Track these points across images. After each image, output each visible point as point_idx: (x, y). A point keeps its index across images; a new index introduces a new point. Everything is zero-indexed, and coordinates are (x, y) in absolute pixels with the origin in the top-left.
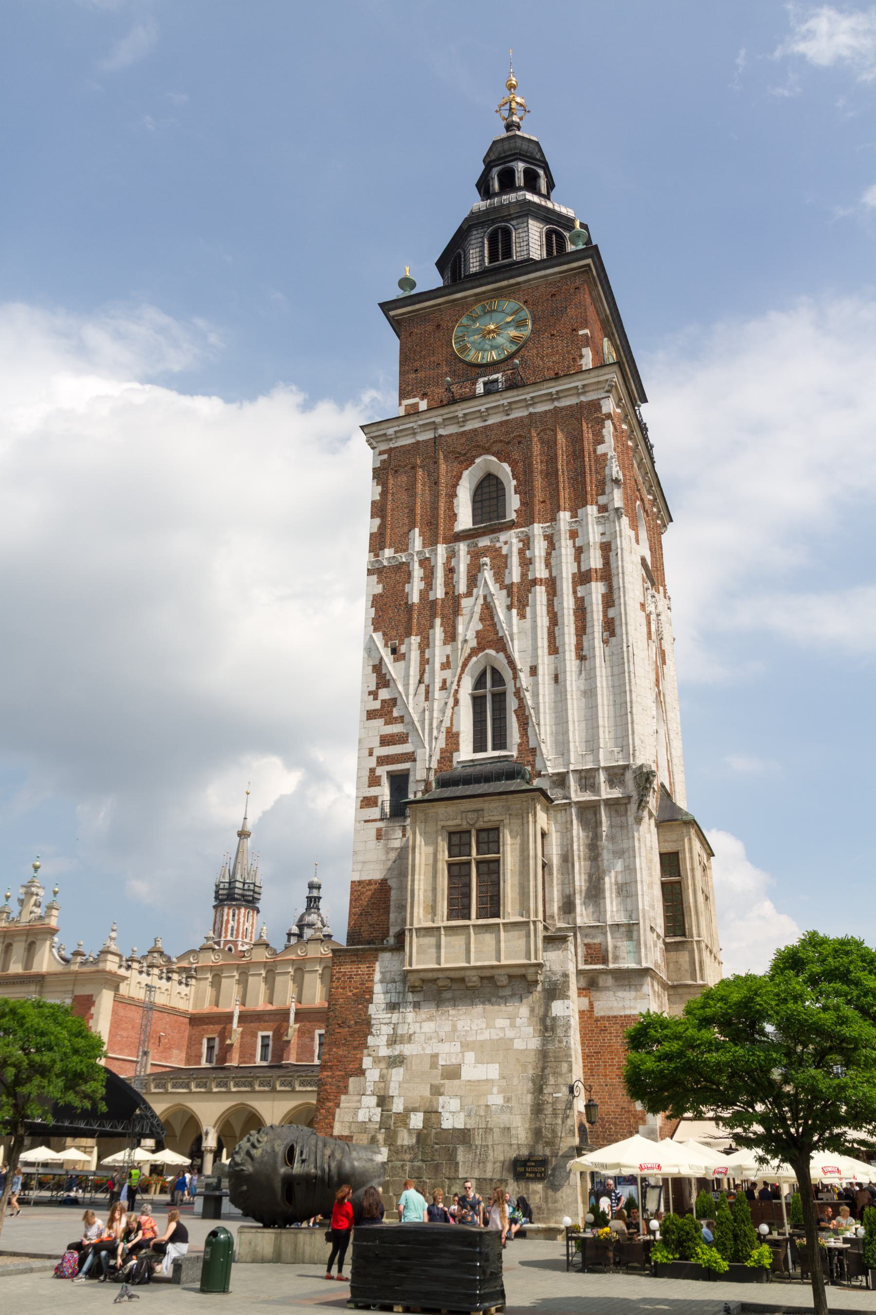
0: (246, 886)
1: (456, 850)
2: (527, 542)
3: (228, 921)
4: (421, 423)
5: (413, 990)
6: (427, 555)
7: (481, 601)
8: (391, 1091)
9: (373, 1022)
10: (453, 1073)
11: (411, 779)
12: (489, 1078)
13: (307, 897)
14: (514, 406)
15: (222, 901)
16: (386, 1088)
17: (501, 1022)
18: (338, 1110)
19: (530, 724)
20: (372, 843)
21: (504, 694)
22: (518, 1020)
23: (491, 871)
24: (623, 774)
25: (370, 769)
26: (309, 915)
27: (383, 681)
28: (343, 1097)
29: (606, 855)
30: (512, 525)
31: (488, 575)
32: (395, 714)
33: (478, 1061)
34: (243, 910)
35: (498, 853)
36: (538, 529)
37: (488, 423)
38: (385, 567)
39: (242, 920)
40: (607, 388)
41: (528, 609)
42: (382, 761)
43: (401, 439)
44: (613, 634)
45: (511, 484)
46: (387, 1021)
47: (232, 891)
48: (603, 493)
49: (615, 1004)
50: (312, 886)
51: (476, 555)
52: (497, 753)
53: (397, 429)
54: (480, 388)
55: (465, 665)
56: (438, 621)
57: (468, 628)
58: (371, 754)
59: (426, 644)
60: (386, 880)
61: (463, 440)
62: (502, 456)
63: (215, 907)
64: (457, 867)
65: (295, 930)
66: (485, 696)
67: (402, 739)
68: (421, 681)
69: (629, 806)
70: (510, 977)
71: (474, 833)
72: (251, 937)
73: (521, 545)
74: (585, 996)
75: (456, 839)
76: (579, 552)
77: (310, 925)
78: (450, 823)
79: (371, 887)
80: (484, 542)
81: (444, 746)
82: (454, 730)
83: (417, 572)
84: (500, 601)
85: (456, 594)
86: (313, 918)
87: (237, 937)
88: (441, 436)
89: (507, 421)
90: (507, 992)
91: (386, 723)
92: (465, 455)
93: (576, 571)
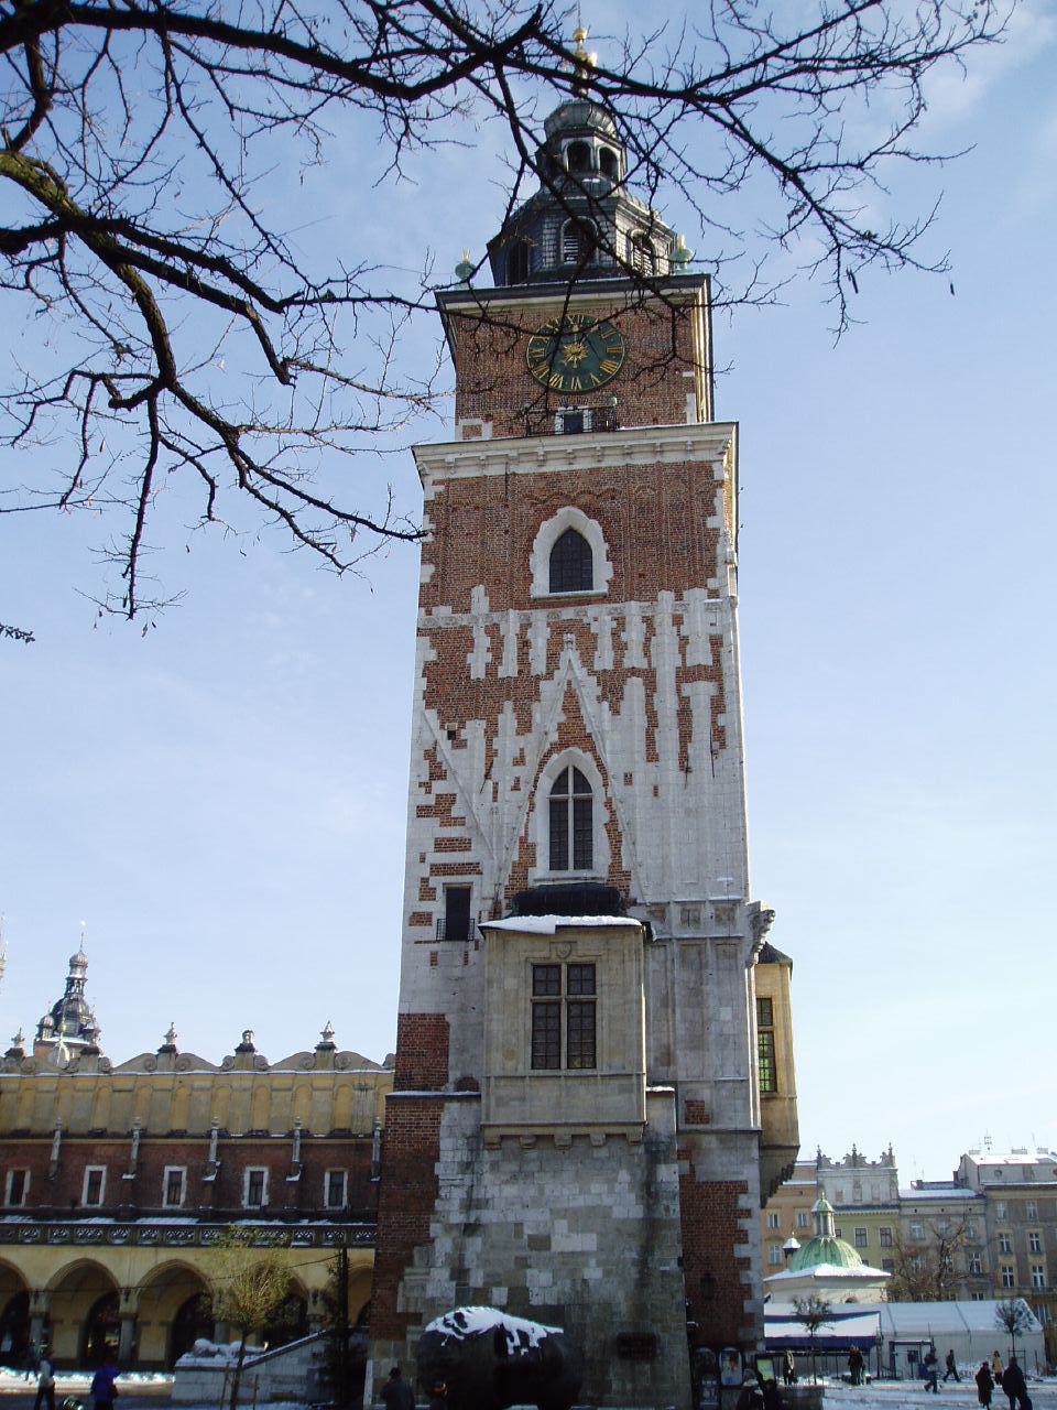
1: (541, 988)
2: (621, 623)
4: (489, 453)
5: (491, 1146)
6: (496, 621)
7: (565, 688)
8: (466, 1263)
9: (441, 1183)
10: (541, 1243)
11: (475, 895)
12: (585, 1248)
13: (68, 979)
14: (607, 452)
16: (461, 1259)
17: (596, 1188)
18: (401, 1284)
19: (624, 842)
20: (425, 968)
21: (590, 801)
22: (617, 1185)
23: (585, 1015)
24: (732, 910)
25: (422, 879)
27: (437, 773)
28: (408, 1270)
29: (711, 1002)
30: (604, 599)
31: (571, 655)
32: (453, 814)
33: (570, 1230)
35: (594, 993)
36: (634, 610)
37: (576, 467)
38: (440, 628)
40: (720, 450)
41: (622, 703)
42: (437, 869)
43: (462, 469)
44: (723, 746)
45: (599, 548)
46: (457, 1182)
48: (714, 575)
49: (720, 1168)
50: (74, 964)
51: (558, 630)
52: (584, 873)
53: (458, 456)
55: (542, 763)
56: (508, 706)
57: (548, 715)
58: (423, 860)
60: (443, 1015)
61: (542, 484)
62: (592, 512)
64: (544, 1007)
66: (567, 801)
67: (463, 845)
68: (487, 776)
69: (738, 948)
70: (608, 1136)
71: (564, 968)
73: (614, 624)
74: (687, 1159)
75: (541, 974)
76: (684, 641)
78: (536, 954)
79: (425, 1022)
80: (568, 614)
81: (516, 859)
82: (530, 840)
83: (483, 641)
84: (589, 690)
85: (533, 673)
88: (514, 474)
89: (599, 468)
90: (603, 1153)
91: (443, 824)
92: (545, 501)
93: (679, 663)
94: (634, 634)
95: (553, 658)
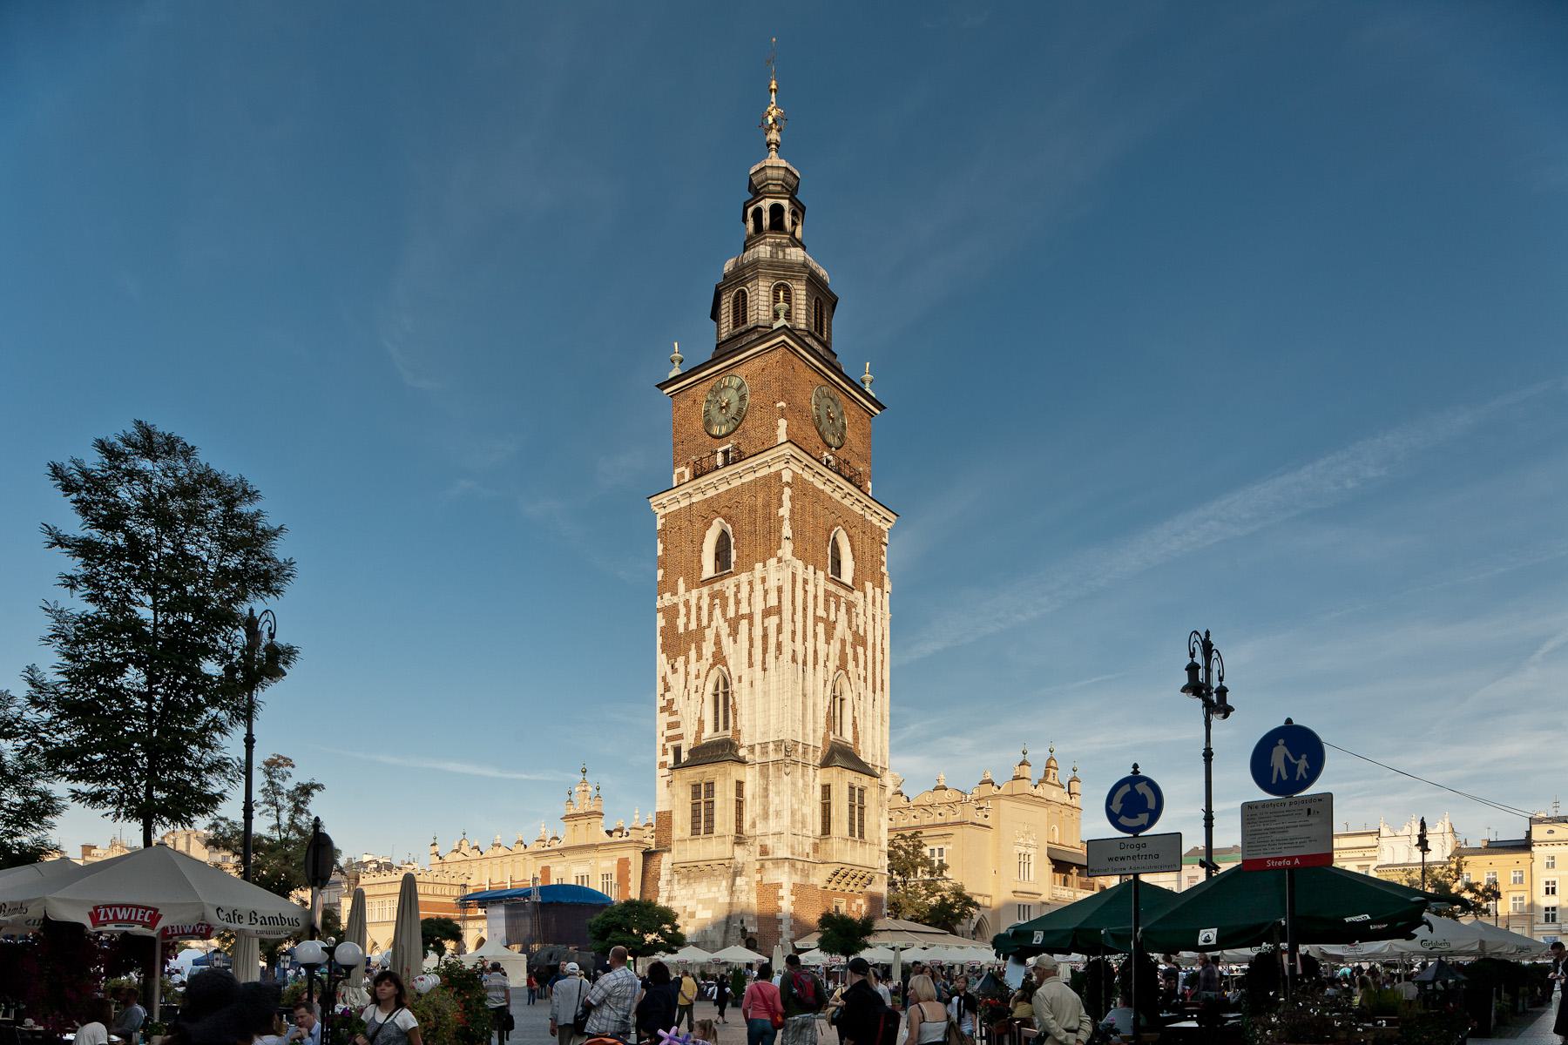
2: (738, 586)
17: (715, 889)
27: (667, 689)
29: (771, 795)
31: (717, 612)
36: (744, 577)
42: (669, 739)
51: (712, 597)
54: (720, 459)
57: (708, 649)
59: (687, 663)
62: (728, 519)
80: (717, 586)
83: (682, 610)
94: (744, 594)
95: (710, 614)
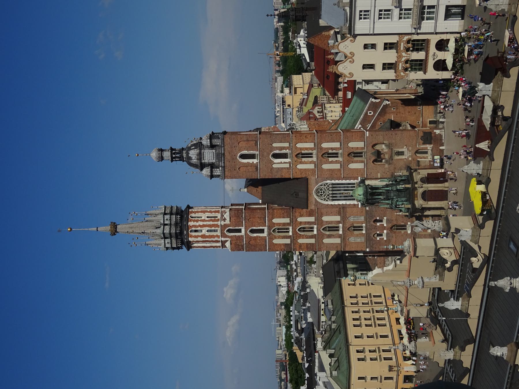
0: (166, 222)
3: (203, 236)
15: (183, 243)
26: (189, 158)
34: (191, 224)
39: (201, 223)
47: (174, 235)
63: (188, 250)
65: (206, 171)
72: (215, 212)
77: (200, 156)
86: (193, 154)
87: (217, 226)
